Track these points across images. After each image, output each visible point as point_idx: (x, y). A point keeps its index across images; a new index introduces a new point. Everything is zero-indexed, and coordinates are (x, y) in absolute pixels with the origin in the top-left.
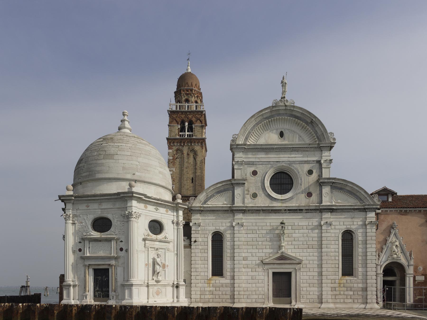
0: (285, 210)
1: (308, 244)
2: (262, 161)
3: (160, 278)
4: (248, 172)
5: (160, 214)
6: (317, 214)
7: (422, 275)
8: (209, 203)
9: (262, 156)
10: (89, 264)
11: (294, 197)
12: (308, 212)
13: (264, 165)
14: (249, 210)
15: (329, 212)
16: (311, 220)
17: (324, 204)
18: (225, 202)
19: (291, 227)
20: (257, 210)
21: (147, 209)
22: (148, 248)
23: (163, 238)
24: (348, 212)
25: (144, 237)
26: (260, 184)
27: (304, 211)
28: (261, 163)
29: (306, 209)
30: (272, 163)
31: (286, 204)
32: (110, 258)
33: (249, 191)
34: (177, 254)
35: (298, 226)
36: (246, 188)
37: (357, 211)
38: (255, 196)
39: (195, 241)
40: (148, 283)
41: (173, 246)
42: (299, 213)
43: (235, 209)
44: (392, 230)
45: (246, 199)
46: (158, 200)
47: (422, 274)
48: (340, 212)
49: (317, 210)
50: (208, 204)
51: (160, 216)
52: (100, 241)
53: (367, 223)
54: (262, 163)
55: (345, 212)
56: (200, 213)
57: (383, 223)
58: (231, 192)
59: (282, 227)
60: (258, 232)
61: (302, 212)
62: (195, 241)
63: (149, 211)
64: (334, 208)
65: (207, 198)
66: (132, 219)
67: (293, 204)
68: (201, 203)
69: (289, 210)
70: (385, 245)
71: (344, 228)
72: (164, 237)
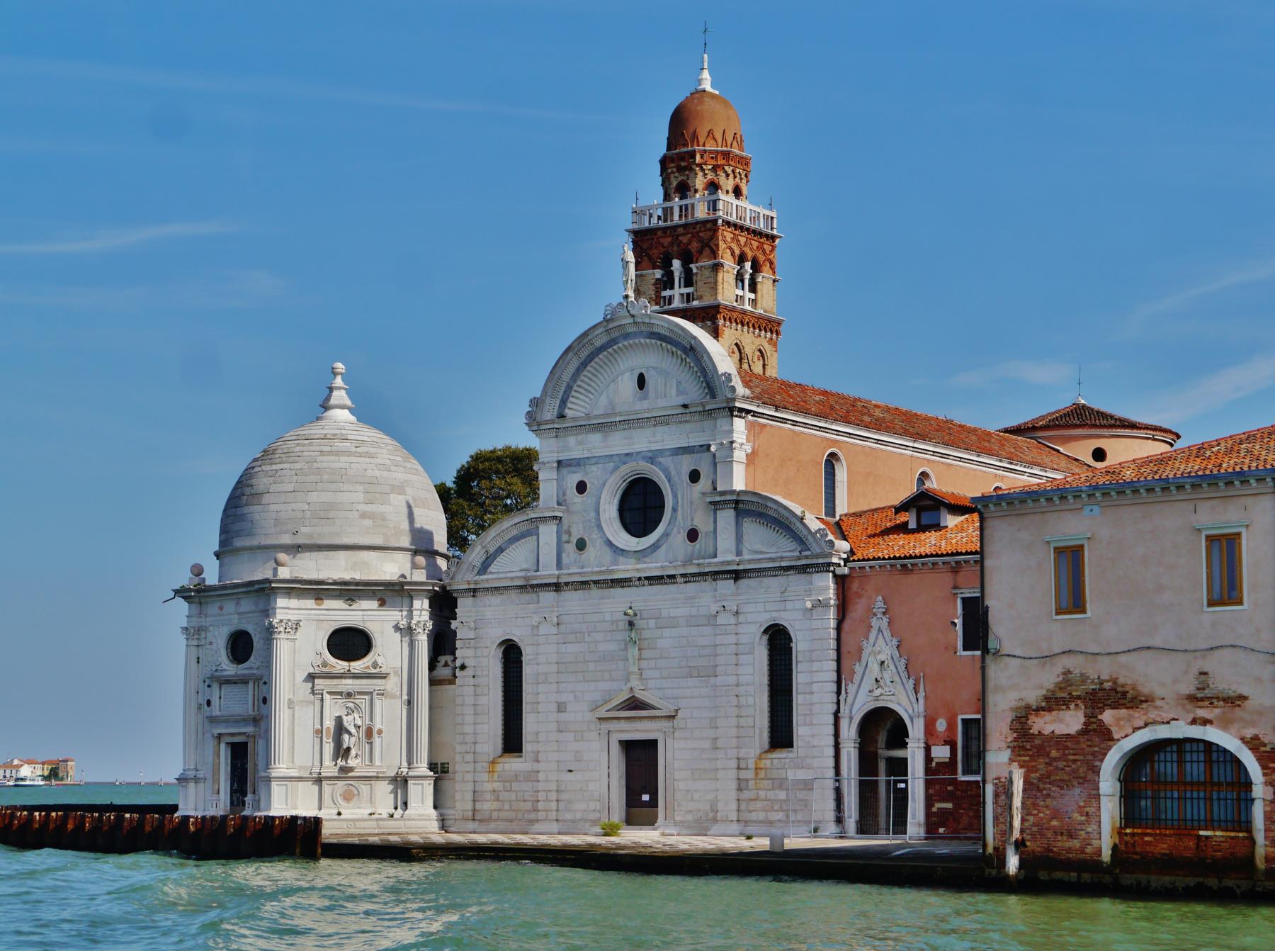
0: (640, 579)
1: (690, 664)
2: (597, 455)
3: (351, 762)
4: (570, 485)
5: (360, 613)
6: (706, 585)
7: (946, 743)
8: (492, 568)
9: (595, 444)
10: (220, 734)
11: (661, 543)
12: (689, 582)
13: (600, 466)
14: (567, 584)
15: (732, 578)
16: (697, 600)
17: (747, 556)
18: (525, 566)
19: (654, 621)
20: (583, 583)
21: (322, 607)
22: (322, 694)
23: (368, 667)
24: (773, 576)
25: (312, 671)
26: (593, 514)
27: (679, 580)
28: (594, 460)
29: (683, 575)
30: (616, 459)
31: (645, 563)
32: (244, 720)
33: (570, 534)
34: (409, 702)
35: (670, 617)
36: (565, 527)
37: (792, 572)
38: (581, 545)
39: (463, 667)
40: (320, 774)
41: (399, 686)
42: (671, 583)
43: (535, 582)
44: (874, 622)
45: (564, 555)
46: (346, 583)
47: (944, 741)
48: (755, 577)
49: (706, 574)
50: (491, 573)
51: (360, 618)
52: (235, 683)
53: (809, 605)
54: (598, 460)
55: (768, 576)
56: (473, 596)
57: (858, 600)
58: (535, 537)
59: (631, 624)
60: (587, 639)
61: (674, 583)
62: (463, 667)
63: (328, 610)
64: (741, 567)
65: (487, 558)
66: (276, 636)
67: (653, 567)
68: (476, 571)
69: (646, 578)
70: (860, 660)
71: (766, 619)
72: (370, 664)
